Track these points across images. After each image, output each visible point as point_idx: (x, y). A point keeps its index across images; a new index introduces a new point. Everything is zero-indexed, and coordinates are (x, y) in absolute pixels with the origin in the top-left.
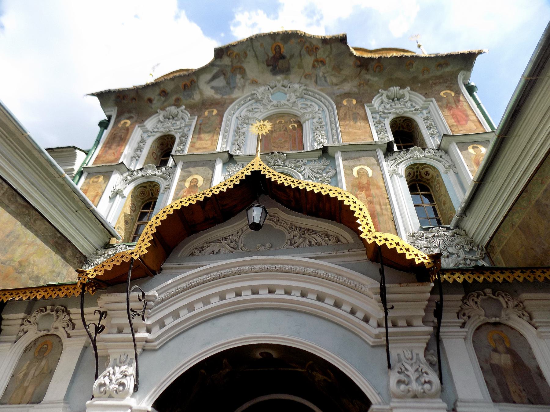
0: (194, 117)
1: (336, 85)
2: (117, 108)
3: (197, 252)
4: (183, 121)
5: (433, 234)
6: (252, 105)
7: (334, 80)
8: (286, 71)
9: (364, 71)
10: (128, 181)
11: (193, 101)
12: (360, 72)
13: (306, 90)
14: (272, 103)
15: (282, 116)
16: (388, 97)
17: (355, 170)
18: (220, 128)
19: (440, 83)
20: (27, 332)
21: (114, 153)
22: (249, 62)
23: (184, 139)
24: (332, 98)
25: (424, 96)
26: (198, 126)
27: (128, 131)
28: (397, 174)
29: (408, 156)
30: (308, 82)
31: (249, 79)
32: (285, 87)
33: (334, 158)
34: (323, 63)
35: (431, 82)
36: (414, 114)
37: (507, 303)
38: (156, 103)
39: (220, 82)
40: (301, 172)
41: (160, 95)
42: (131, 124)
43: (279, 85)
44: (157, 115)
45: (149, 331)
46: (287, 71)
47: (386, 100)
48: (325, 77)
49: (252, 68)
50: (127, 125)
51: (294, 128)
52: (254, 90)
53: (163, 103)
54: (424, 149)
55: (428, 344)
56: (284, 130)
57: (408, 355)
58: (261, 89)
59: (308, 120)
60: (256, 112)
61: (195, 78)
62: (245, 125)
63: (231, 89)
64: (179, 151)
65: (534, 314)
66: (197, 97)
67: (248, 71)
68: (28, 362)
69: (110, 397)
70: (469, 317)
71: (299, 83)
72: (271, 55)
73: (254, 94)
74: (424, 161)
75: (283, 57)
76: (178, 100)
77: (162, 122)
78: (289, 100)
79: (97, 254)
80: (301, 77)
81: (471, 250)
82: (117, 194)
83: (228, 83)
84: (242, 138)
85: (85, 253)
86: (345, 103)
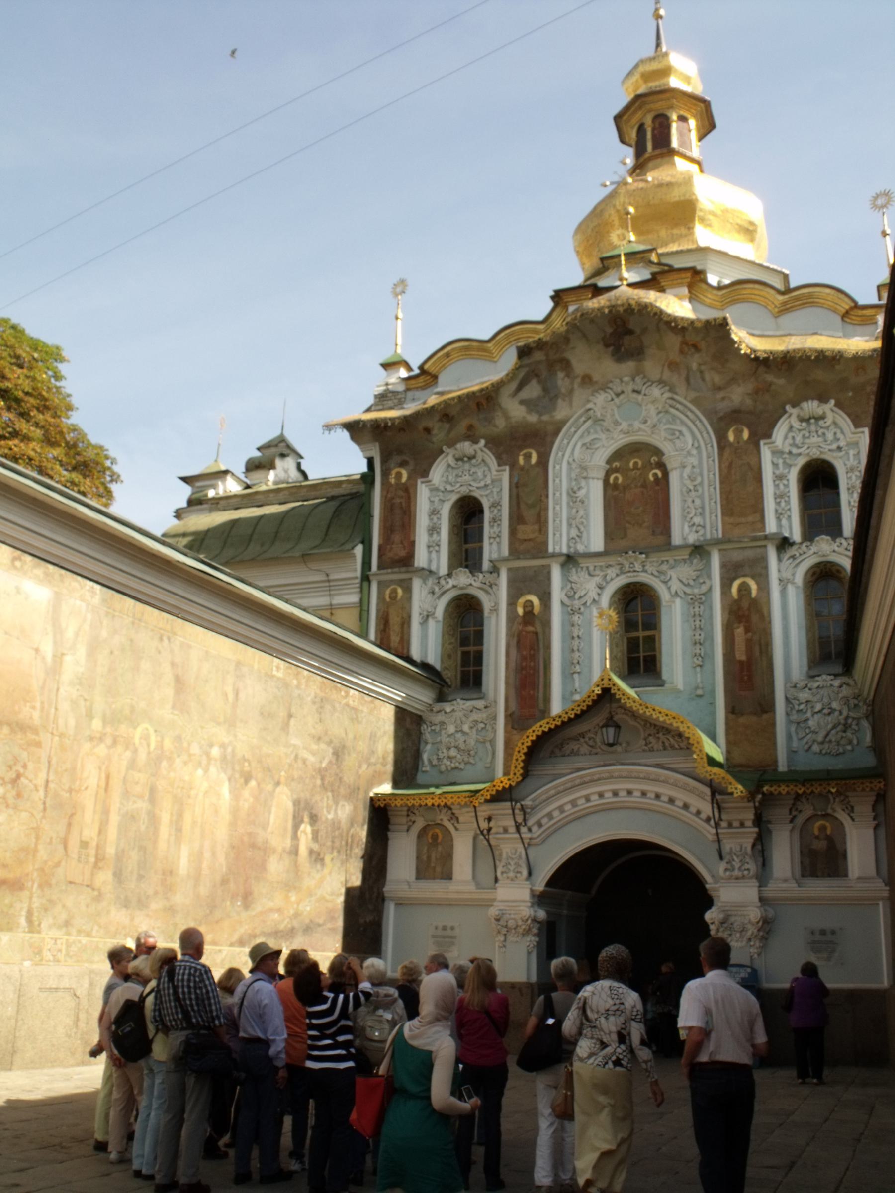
1: (720, 389)
2: (377, 445)
4: (486, 469)
5: (818, 684)
6: (588, 431)
7: (717, 379)
8: (637, 353)
9: (762, 369)
10: (436, 596)
12: (757, 369)
13: (672, 399)
14: (620, 428)
16: (802, 420)
17: (736, 584)
18: (547, 496)
20: (414, 822)
21: (402, 543)
22: (573, 348)
24: (711, 425)
26: (514, 490)
27: (408, 493)
28: (793, 583)
29: (812, 552)
30: (675, 379)
31: (576, 377)
32: (638, 392)
33: (708, 554)
34: (695, 347)
36: (835, 458)
37: (834, 799)
38: (439, 433)
39: (533, 390)
40: (665, 582)
41: (440, 420)
42: (409, 478)
44: (443, 456)
45: (530, 830)
46: (639, 354)
47: (796, 424)
48: (701, 372)
49: (583, 359)
52: (588, 401)
53: (449, 432)
54: (834, 540)
58: (601, 398)
59: (676, 469)
60: (597, 449)
61: (493, 394)
63: (551, 400)
64: (494, 538)
65: (856, 809)
66: (500, 423)
67: (574, 362)
68: (426, 848)
70: (800, 811)
71: (661, 382)
72: (609, 330)
73: (590, 409)
75: (630, 332)
76: (470, 427)
77: (453, 468)
78: (645, 422)
79: (432, 710)
80: (663, 366)
81: (856, 706)
82: (428, 616)
83: (545, 390)
85: (419, 713)
86: (731, 437)
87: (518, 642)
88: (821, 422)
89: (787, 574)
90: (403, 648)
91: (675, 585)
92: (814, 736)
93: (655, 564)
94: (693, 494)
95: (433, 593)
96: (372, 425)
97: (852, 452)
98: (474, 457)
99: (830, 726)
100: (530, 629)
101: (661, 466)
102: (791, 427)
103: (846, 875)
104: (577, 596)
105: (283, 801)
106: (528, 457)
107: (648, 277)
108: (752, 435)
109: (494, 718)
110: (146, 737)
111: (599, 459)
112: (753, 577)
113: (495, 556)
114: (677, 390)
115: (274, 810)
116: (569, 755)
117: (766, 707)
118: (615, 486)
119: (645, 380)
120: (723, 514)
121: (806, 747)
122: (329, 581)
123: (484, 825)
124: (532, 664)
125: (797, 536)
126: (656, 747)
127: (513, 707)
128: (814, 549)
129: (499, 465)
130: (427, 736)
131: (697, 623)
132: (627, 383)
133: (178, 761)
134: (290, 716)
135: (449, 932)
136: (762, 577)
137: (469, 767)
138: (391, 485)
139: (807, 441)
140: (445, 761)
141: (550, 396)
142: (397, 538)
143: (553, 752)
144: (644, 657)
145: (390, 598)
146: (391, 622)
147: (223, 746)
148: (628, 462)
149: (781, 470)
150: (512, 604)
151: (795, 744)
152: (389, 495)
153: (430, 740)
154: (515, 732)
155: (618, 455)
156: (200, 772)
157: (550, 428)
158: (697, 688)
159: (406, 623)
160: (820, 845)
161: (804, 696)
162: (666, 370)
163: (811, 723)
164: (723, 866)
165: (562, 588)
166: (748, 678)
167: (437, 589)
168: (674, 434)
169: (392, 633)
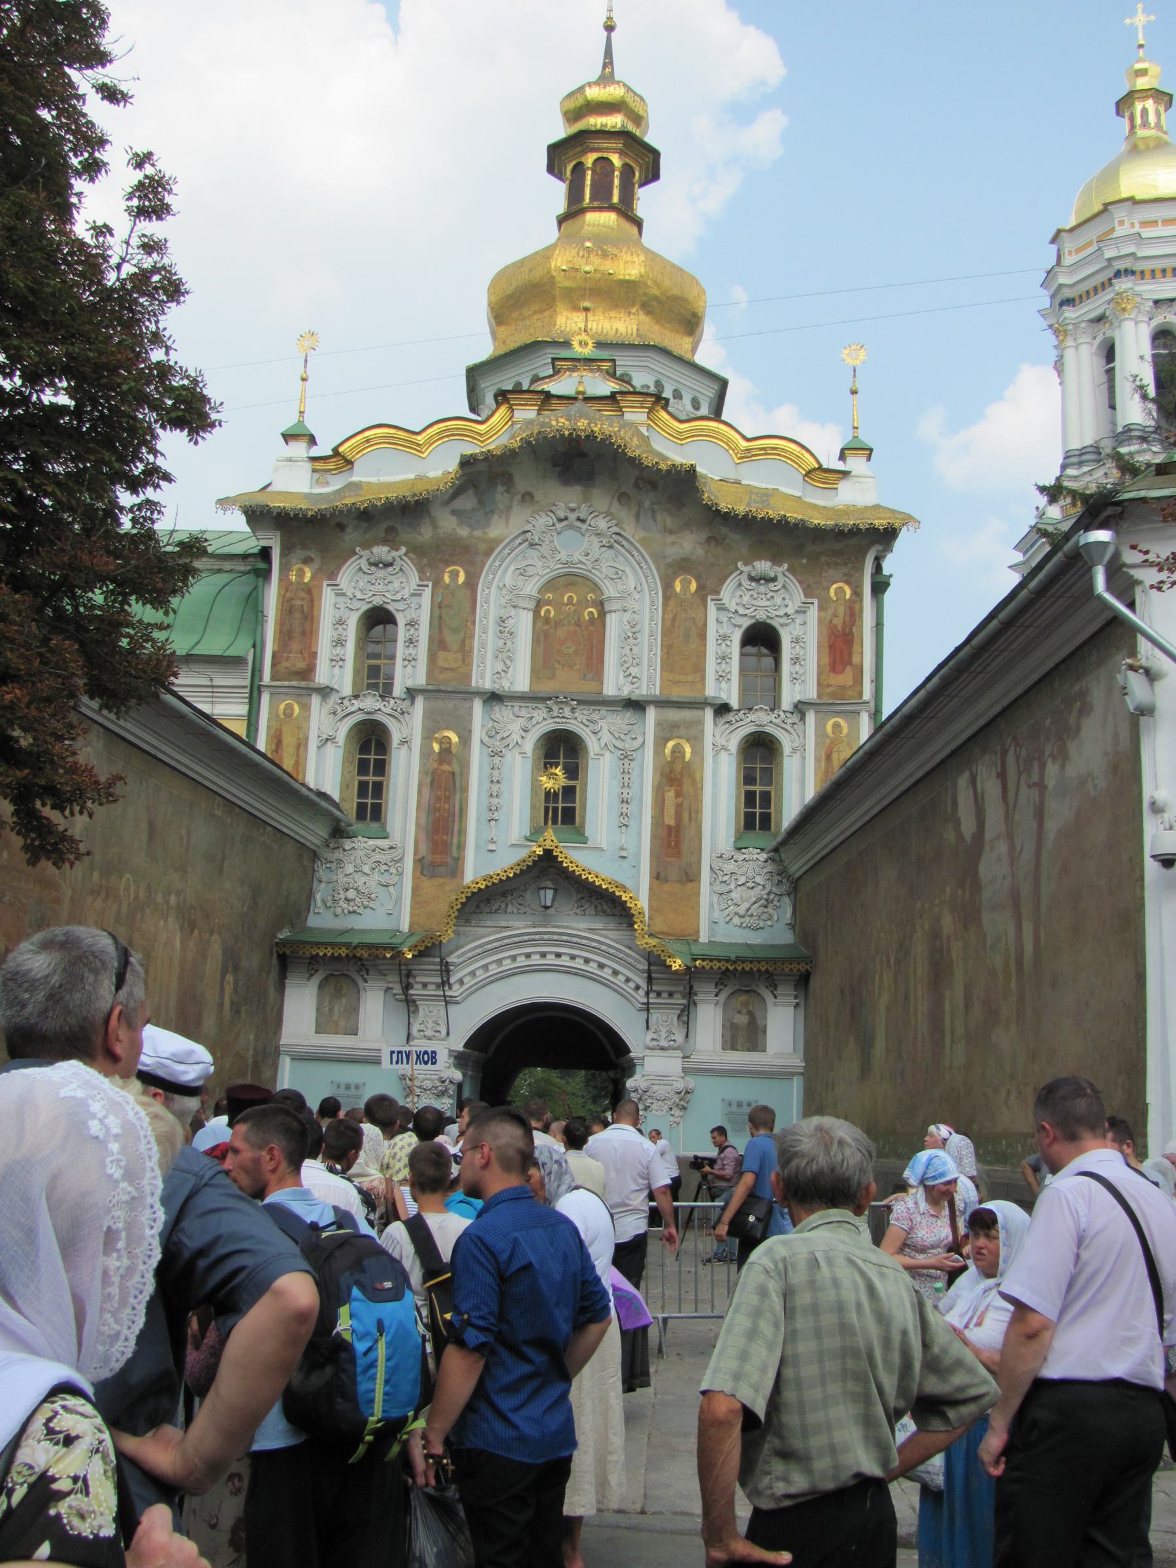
0: (425, 583)
1: (671, 532)
2: (279, 534)
3: (482, 906)
7: (669, 521)
11: (420, 538)
15: (573, 584)
17: (670, 744)
19: (836, 564)
23: (412, 630)
24: (658, 569)
25: (803, 590)
27: (311, 594)
29: (749, 720)
32: (583, 521)
34: (653, 485)
35: (823, 559)
36: (782, 625)
39: (467, 502)
43: (572, 517)
47: (746, 583)
48: (653, 511)
50: (306, 580)
51: (592, 618)
54: (772, 710)
55: (682, 1011)
56: (578, 624)
57: (665, 1018)
58: (543, 521)
62: (513, 612)
63: (486, 514)
69: (429, 1039)
71: (608, 514)
74: (770, 729)
75: (583, 455)
78: (587, 554)
79: (328, 846)
83: (481, 503)
84: (508, 642)
85: (313, 847)
86: (678, 587)
87: (432, 782)
88: (772, 585)
89: (721, 741)
90: (298, 773)
91: (606, 737)
92: (737, 909)
93: (585, 712)
94: (631, 641)
95: (334, 713)
96: (279, 514)
97: (799, 621)
98: (391, 564)
99: (753, 900)
100: (446, 767)
101: (600, 605)
102: (740, 585)
103: (765, 1051)
104: (498, 737)
105: (216, 949)
106: (455, 575)
107: (609, 394)
108: (700, 588)
109: (401, 859)
110: (127, 889)
111: (531, 588)
112: (688, 741)
113: (410, 684)
114: (625, 526)
115: (209, 959)
116: (496, 912)
117: (690, 877)
118: (547, 620)
119: (592, 509)
120: (662, 668)
121: (728, 919)
122: (212, 686)
123: (404, 979)
124: (447, 806)
125: (735, 704)
126: (587, 912)
127: (423, 850)
128: (752, 717)
129: (421, 580)
130: (321, 872)
131: (626, 779)
132: (573, 510)
133: (148, 911)
134: (224, 858)
135: (353, 1091)
136: (697, 741)
137: (368, 911)
138: (292, 583)
139: (755, 603)
140: (341, 903)
141: (486, 509)
142: (295, 646)
143: (478, 907)
144: (563, 808)
145: (284, 714)
146: (285, 742)
147: (178, 894)
148: (562, 596)
149: (725, 629)
150: (428, 737)
151: (717, 915)
152: (288, 595)
153: (324, 879)
154: (424, 878)
155: (550, 585)
156: (162, 923)
157: (482, 547)
158: (622, 849)
159: (301, 745)
160: (742, 1020)
161: (729, 867)
162: (615, 503)
163: (733, 895)
164: (650, 1035)
165: (483, 726)
166: (674, 843)
167: (339, 710)
168: (617, 573)
169: (285, 755)
